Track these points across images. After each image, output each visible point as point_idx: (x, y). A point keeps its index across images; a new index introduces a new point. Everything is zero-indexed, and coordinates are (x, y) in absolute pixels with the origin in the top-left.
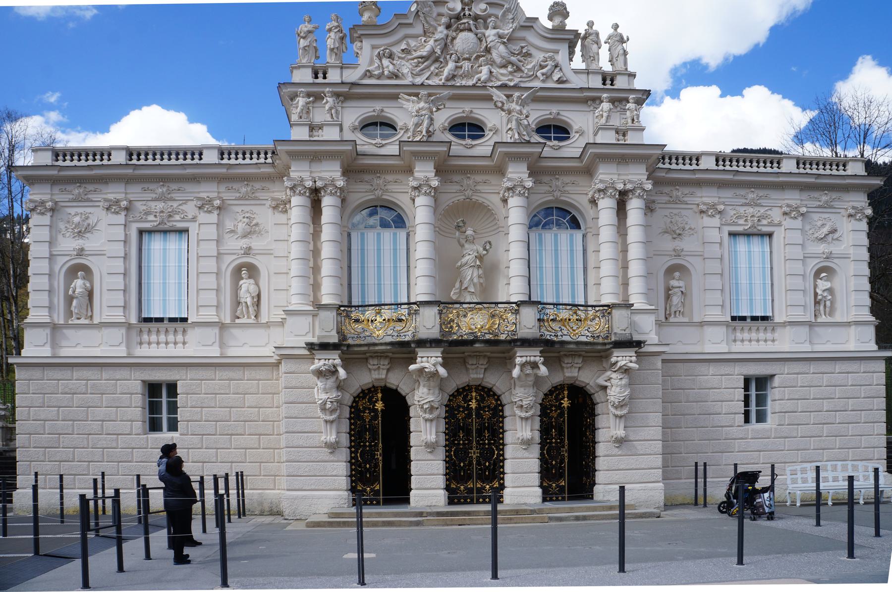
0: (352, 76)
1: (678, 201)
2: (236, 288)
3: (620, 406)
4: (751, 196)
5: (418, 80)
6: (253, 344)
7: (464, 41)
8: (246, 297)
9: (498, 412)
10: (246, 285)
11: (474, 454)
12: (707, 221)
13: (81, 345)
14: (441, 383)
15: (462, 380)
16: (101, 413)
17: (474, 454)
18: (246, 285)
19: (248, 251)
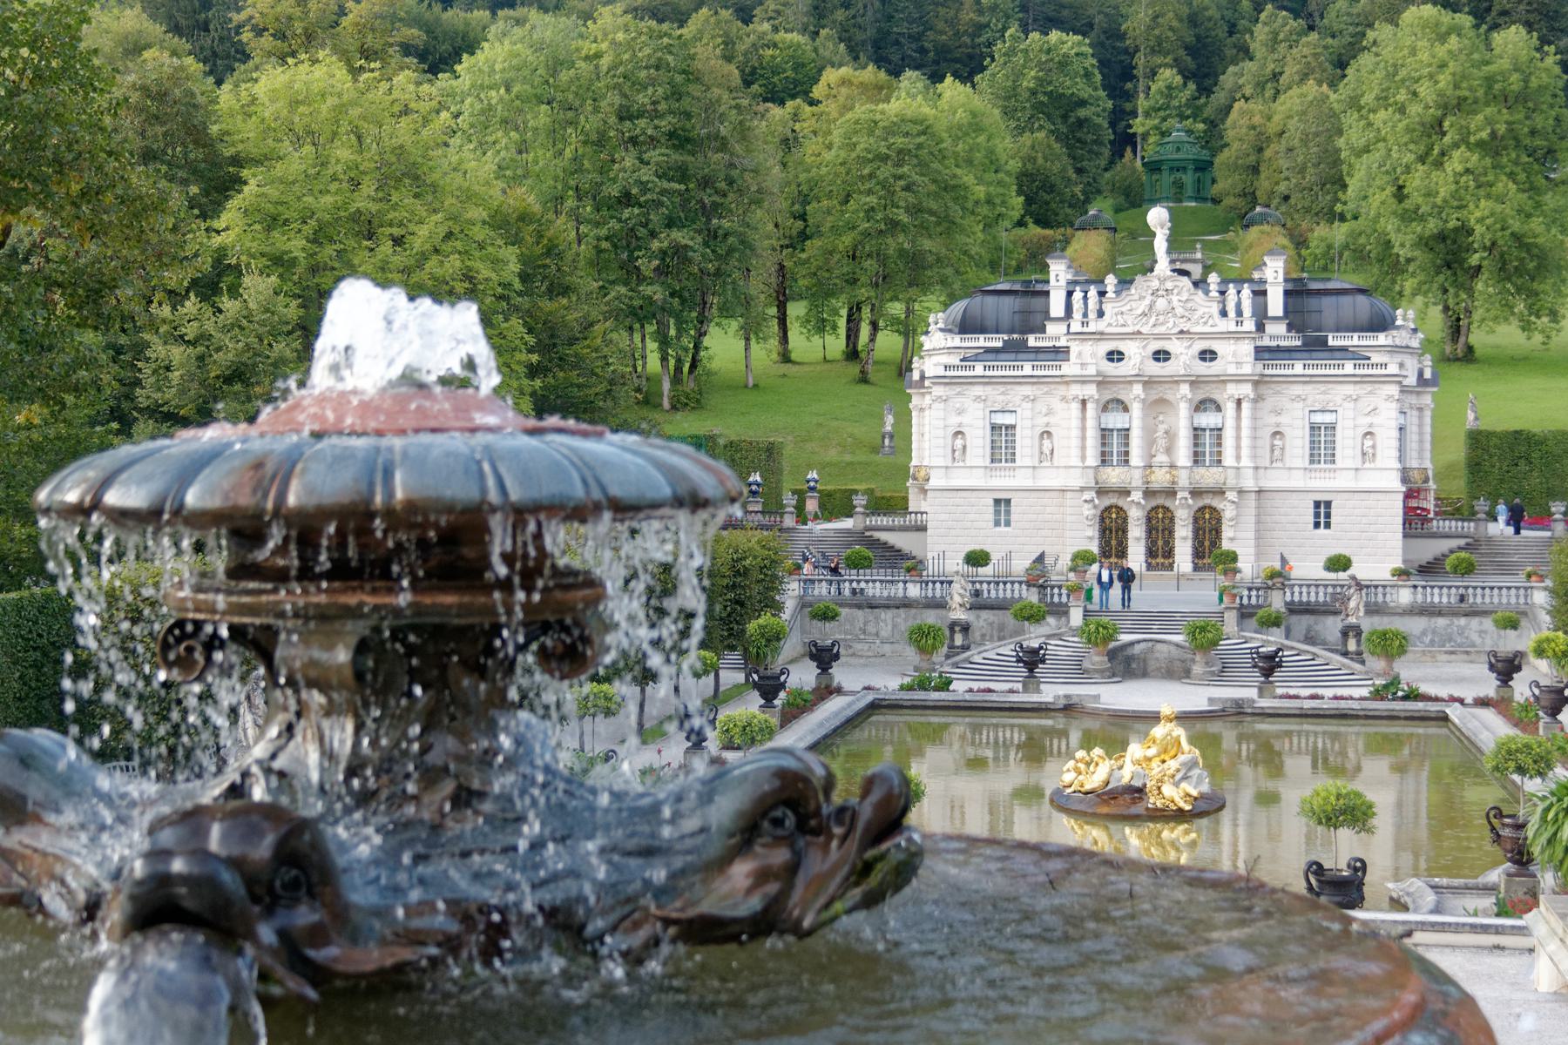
0: (1101, 325)
1: (1278, 393)
2: (1041, 445)
3: (1231, 520)
4: (1322, 387)
5: (1137, 328)
6: (1050, 479)
7: (1161, 303)
8: (1047, 451)
9: (1172, 519)
10: (1046, 442)
11: (1160, 543)
12: (1296, 405)
13: (960, 479)
14: (1143, 507)
15: (1154, 504)
16: (972, 516)
17: (1160, 543)
18: (1046, 442)
19: (1047, 425)
